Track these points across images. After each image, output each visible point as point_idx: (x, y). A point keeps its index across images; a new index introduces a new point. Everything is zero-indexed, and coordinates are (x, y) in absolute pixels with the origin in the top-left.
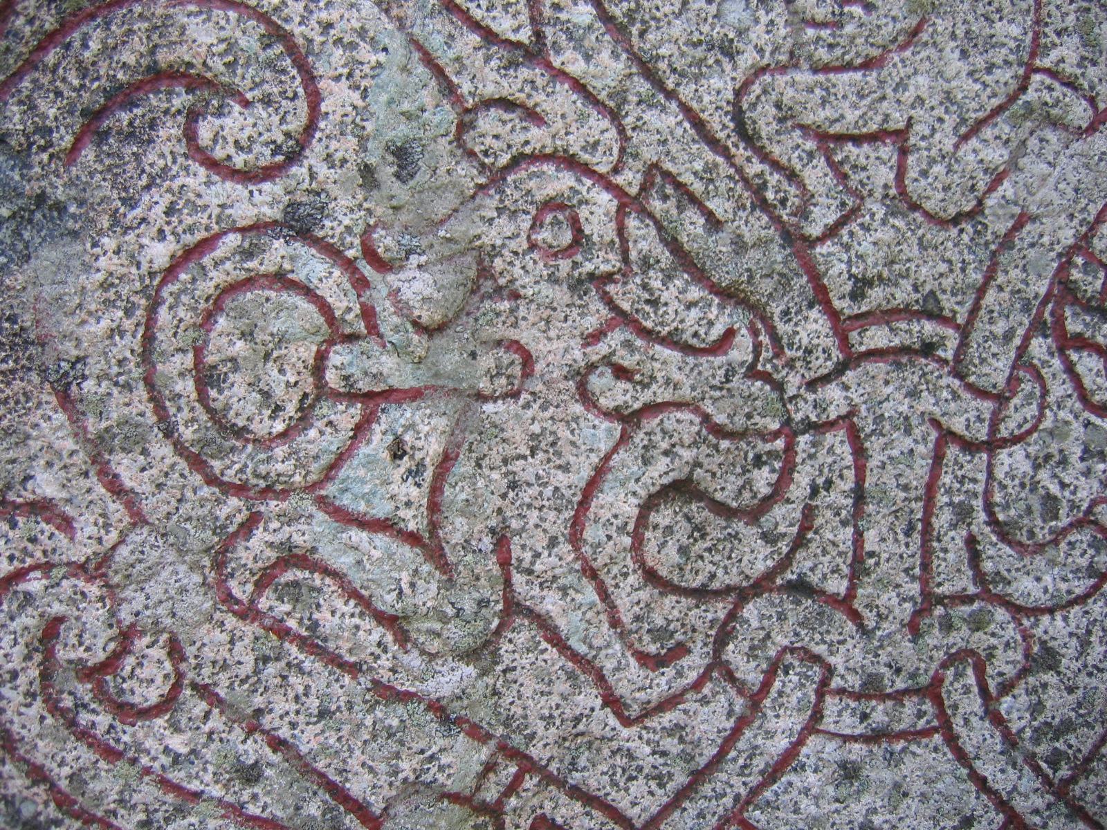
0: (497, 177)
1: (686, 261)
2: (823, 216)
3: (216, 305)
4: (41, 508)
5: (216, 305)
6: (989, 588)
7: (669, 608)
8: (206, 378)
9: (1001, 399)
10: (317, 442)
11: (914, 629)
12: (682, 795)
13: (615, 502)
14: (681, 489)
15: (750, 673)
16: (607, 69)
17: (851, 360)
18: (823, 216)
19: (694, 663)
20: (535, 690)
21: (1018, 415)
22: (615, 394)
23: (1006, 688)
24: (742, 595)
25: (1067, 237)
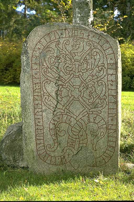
0: (61, 54)
1: (68, 57)
2: (74, 56)
3: (51, 59)
4: (44, 66)
5: (51, 59)
6: (81, 72)
7: (67, 71)
8: (50, 61)
9: (82, 63)
10: (54, 63)
11: (78, 73)
12: (68, 79)
13: (65, 66)
14: (68, 66)
15: (71, 74)
16: (65, 50)
17: (75, 61)
18: (74, 56)
19: (68, 73)
20: (62, 74)
21: (83, 64)
22: (65, 62)
23: (82, 76)
24: (70, 71)
25: (85, 57)
